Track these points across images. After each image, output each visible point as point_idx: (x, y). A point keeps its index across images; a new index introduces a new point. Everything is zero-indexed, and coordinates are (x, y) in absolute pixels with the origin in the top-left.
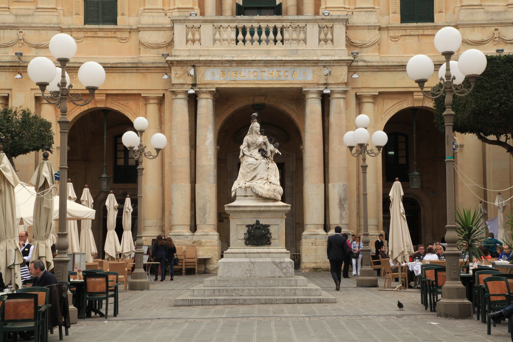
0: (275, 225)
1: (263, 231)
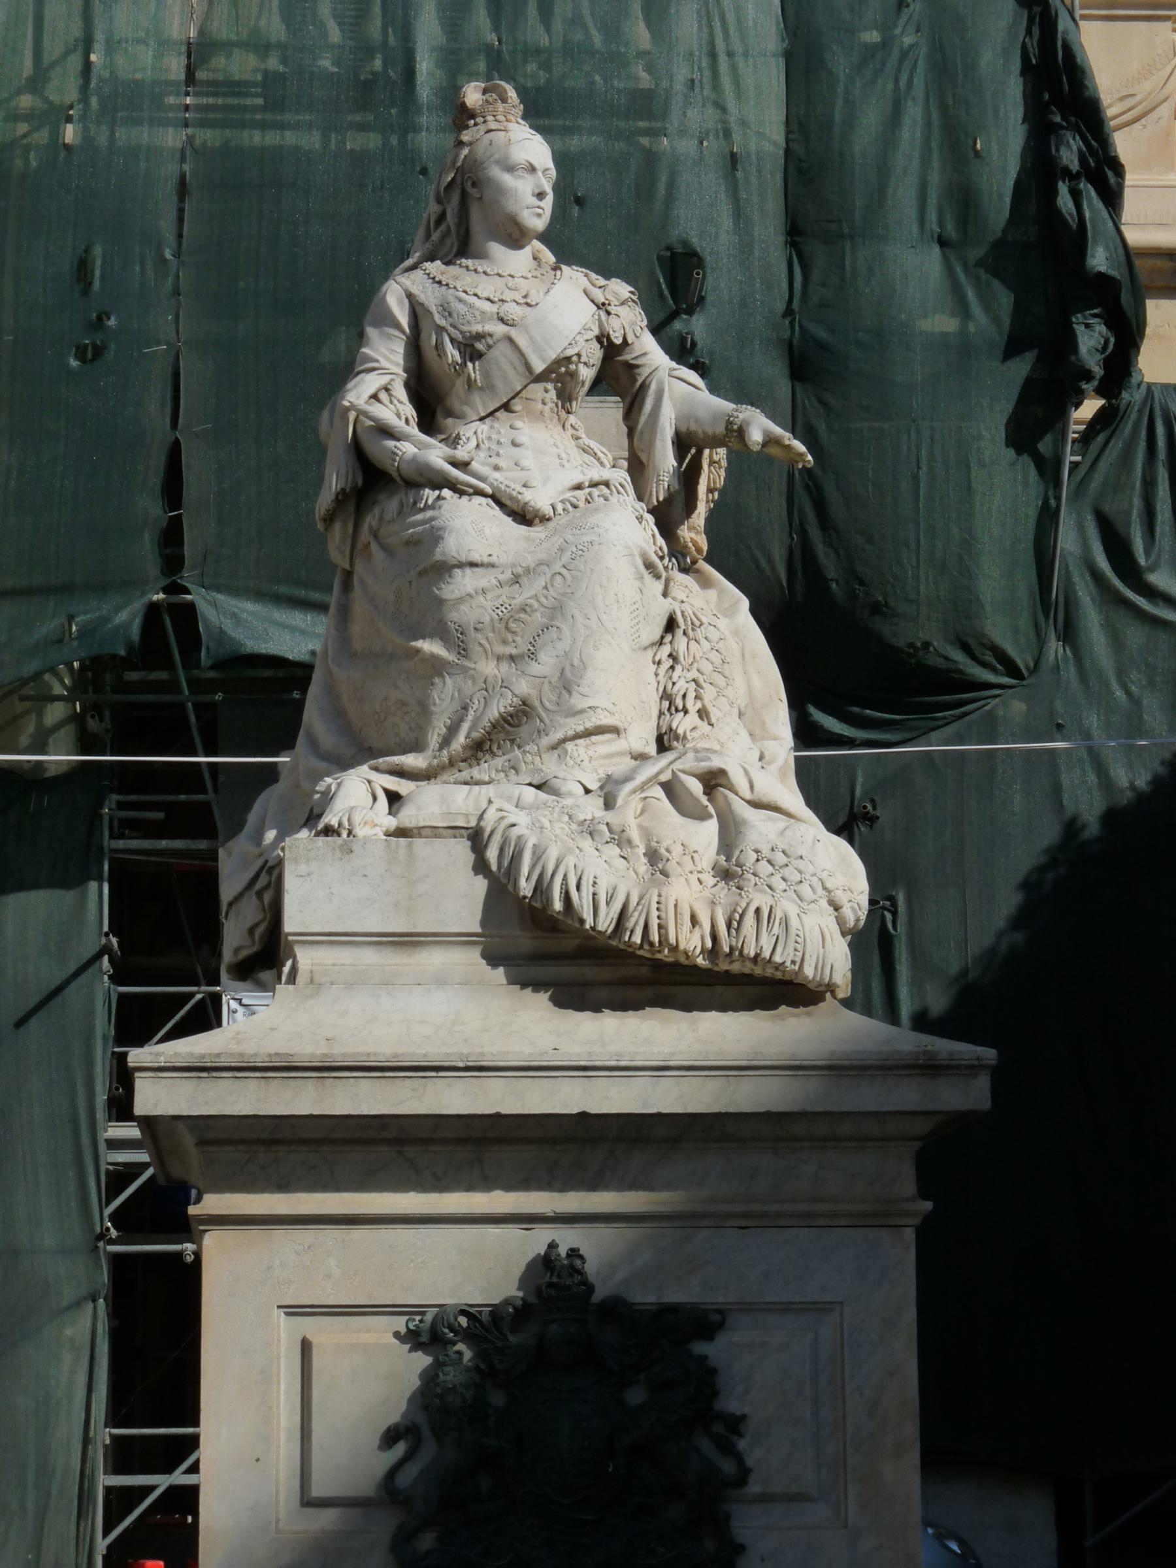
0: (787, 1308)
1: (636, 1396)
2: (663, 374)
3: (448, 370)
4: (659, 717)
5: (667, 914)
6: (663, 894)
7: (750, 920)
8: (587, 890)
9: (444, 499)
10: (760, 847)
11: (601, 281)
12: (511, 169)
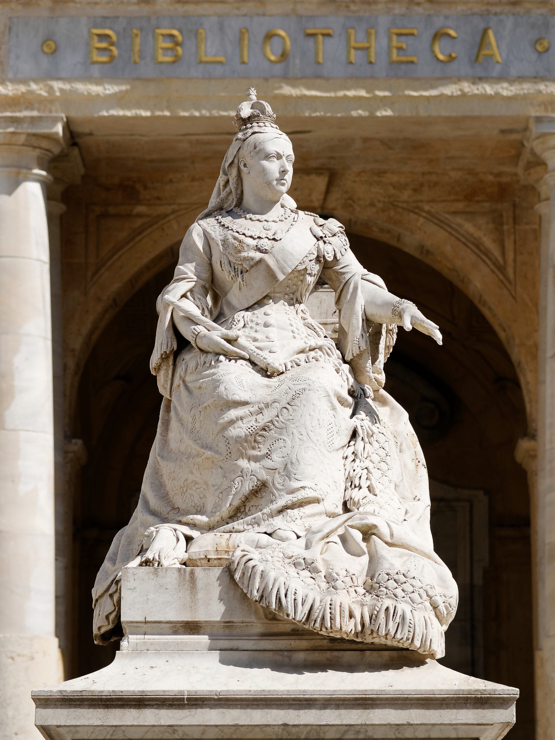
2: (358, 278)
3: (228, 279)
4: (345, 490)
5: (335, 611)
6: (333, 599)
7: (382, 615)
8: (291, 597)
9: (221, 362)
10: (390, 572)
11: (321, 221)
12: (267, 157)
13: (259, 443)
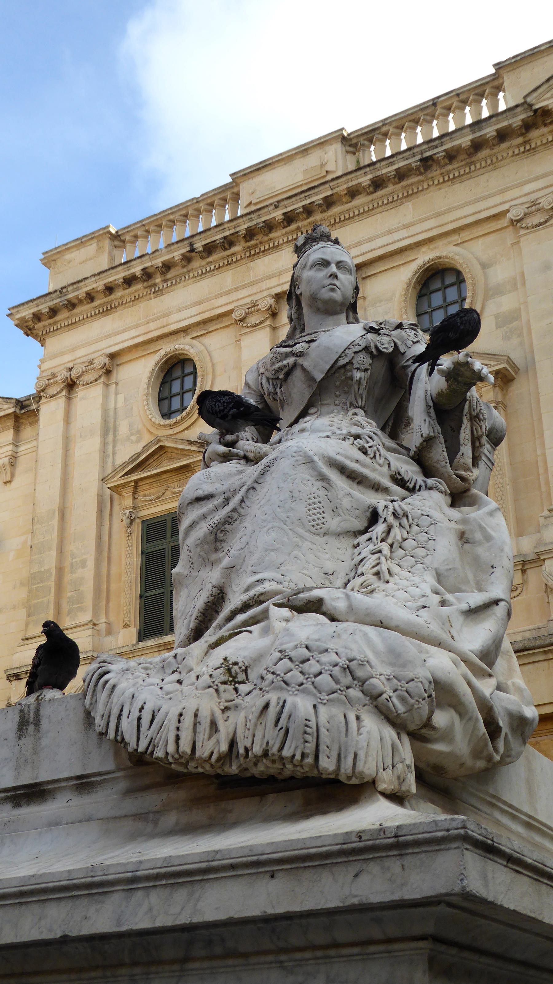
13: (222, 541)
